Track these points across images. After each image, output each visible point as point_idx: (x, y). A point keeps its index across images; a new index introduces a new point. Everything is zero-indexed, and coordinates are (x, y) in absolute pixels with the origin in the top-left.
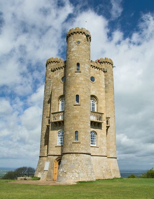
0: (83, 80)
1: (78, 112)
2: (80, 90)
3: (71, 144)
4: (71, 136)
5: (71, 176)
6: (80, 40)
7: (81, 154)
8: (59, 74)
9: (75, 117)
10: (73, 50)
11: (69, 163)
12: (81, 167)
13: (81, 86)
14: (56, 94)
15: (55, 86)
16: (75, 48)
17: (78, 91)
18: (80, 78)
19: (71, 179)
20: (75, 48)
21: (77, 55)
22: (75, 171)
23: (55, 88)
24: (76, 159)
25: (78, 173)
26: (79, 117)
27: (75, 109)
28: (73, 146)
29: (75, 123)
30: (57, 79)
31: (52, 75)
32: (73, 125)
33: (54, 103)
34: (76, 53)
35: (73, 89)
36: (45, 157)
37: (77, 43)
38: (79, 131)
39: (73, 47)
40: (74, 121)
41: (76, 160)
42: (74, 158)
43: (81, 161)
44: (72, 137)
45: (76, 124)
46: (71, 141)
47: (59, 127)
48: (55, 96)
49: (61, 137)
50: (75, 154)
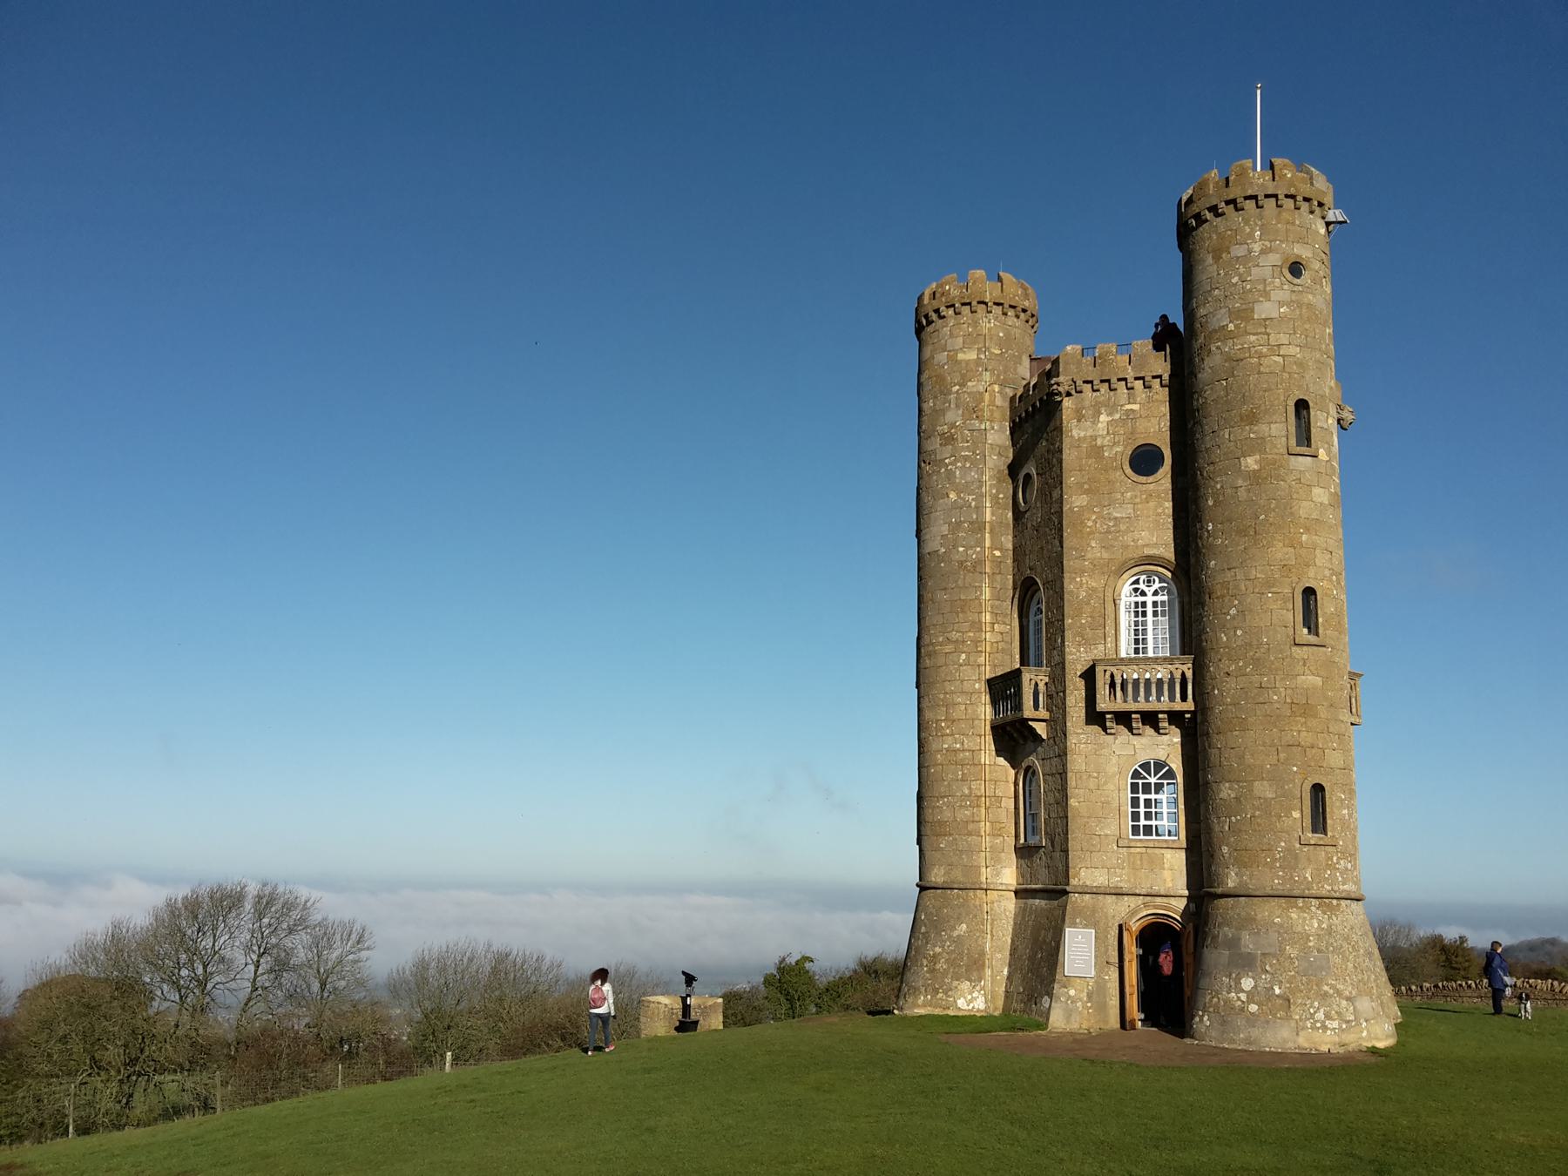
1: (1318, 681)
3: (1289, 850)
4: (1290, 809)
5: (1320, 1015)
6: (1302, 252)
7: (1343, 903)
8: (1103, 418)
9: (1303, 708)
10: (1264, 310)
13: (1320, 540)
15: (1087, 492)
16: (1280, 304)
17: (1308, 566)
18: (1316, 491)
19: (1325, 1028)
20: (1280, 304)
21: (1293, 350)
22: (1332, 987)
23: (1089, 508)
25: (1348, 999)
26: (1323, 713)
27: (1299, 668)
29: (1306, 738)
30: (1096, 451)
31: (987, 396)
34: (1284, 339)
35: (1280, 551)
41: (1330, 931)
44: (1296, 814)
49: (1153, 796)
50: (1314, 901)
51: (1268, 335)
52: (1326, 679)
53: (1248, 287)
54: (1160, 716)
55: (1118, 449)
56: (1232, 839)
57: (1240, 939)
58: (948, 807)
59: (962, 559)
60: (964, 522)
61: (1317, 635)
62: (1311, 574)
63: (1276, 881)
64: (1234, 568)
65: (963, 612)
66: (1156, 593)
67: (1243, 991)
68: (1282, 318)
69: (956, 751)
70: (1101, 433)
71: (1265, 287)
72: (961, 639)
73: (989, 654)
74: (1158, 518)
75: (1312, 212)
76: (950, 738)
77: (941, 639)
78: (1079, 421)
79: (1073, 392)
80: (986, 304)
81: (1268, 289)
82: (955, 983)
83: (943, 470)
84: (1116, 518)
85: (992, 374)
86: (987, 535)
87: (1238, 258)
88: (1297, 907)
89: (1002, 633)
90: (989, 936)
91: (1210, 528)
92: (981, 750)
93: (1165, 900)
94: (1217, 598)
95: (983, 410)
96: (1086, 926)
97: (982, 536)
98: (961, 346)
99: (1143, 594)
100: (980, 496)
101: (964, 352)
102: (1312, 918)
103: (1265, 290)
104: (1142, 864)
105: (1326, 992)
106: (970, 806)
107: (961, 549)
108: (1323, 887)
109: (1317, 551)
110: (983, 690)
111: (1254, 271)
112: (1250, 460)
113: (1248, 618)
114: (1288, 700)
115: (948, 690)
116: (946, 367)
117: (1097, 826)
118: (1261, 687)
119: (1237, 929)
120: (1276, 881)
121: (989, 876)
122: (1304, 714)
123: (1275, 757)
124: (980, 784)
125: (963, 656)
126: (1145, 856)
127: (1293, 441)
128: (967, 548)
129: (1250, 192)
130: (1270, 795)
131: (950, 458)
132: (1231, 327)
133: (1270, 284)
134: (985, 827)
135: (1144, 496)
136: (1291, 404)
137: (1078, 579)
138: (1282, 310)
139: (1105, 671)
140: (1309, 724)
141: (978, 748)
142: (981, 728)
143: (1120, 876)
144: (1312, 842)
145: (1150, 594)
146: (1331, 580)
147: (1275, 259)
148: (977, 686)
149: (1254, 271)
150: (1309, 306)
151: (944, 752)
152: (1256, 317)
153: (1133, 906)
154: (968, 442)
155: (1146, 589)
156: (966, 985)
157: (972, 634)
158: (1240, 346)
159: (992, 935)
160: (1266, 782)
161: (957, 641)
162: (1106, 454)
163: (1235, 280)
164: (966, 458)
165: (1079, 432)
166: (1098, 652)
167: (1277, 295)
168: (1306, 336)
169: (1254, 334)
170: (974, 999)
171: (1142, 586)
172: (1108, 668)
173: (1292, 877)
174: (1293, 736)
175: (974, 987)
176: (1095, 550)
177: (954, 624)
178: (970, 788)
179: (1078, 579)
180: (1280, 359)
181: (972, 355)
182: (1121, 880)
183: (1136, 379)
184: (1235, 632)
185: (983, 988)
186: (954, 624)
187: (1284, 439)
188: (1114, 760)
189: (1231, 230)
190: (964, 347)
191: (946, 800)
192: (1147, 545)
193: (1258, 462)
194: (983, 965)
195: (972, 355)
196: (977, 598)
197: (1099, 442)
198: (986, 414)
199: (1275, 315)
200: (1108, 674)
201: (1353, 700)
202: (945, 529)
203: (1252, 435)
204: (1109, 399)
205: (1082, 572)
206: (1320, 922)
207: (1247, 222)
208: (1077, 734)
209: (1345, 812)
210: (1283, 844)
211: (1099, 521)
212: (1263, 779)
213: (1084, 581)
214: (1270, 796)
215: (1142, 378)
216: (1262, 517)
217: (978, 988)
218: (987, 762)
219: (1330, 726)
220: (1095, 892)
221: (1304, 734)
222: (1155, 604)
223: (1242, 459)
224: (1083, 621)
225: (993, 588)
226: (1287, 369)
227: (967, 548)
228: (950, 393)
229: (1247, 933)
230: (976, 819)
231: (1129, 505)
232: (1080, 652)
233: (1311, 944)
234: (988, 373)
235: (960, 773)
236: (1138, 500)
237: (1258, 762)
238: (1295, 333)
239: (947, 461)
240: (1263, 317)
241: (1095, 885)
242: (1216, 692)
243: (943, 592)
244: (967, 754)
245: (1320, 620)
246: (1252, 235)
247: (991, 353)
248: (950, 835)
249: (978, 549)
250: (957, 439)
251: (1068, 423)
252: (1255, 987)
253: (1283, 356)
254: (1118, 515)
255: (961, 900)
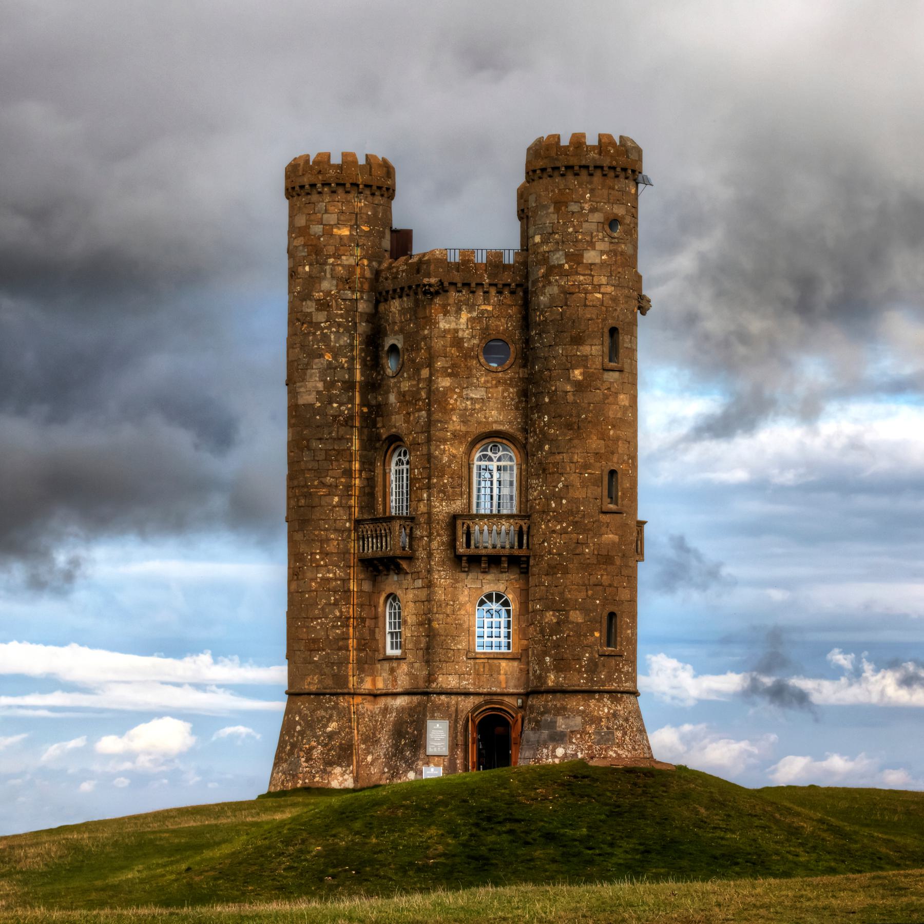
0: (627, 404)
2: (620, 451)
3: (590, 660)
7: (625, 696)
8: (464, 316)
10: (591, 256)
11: (594, 726)
12: (630, 739)
14: (454, 418)
15: (450, 375)
16: (602, 253)
17: (613, 453)
20: (602, 253)
21: (609, 289)
22: (616, 752)
23: (451, 389)
24: (612, 711)
26: (618, 561)
27: (604, 529)
28: (600, 668)
30: (457, 342)
31: (358, 270)
32: (598, 588)
33: (445, 459)
34: (604, 280)
36: (349, 694)
37: (607, 228)
38: (618, 613)
39: (592, 245)
40: (602, 575)
41: (615, 715)
42: (606, 710)
43: (627, 720)
44: (597, 634)
45: (610, 586)
46: (590, 647)
47: (481, 576)
48: (451, 427)
51: (593, 276)
52: (621, 537)
53: (580, 237)
54: (503, 559)
55: (475, 342)
56: (553, 652)
57: (556, 722)
58: (321, 626)
59: (336, 414)
60: (338, 381)
61: (616, 504)
62: (615, 460)
63: (582, 681)
64: (563, 453)
65: (337, 460)
66: (499, 460)
67: (556, 757)
68: (603, 264)
69: (329, 579)
70: (462, 327)
71: (592, 238)
72: (334, 484)
73: (358, 497)
74: (504, 400)
75: (627, 178)
76: (324, 569)
77: (316, 483)
78: (445, 315)
79: (441, 291)
80: (358, 185)
81: (594, 240)
82: (329, 769)
83: (318, 333)
84: (472, 399)
85: (362, 249)
86: (357, 394)
87: (573, 213)
88: (595, 699)
89: (367, 479)
90: (356, 732)
91: (546, 419)
92: (350, 579)
93: (500, 698)
94: (550, 474)
95: (354, 282)
96: (443, 718)
97: (353, 394)
98: (336, 222)
99: (490, 459)
100: (352, 359)
101: (339, 229)
102: (604, 706)
103: (591, 241)
104: (484, 671)
105: (611, 756)
106: (341, 626)
107: (335, 405)
108: (612, 685)
109: (620, 442)
110: (352, 528)
111: (585, 225)
112: (577, 372)
113: (571, 491)
114: (596, 553)
115: (322, 528)
116: (322, 239)
117: (451, 643)
118: (578, 543)
119: (554, 715)
120: (582, 681)
121: (355, 684)
122: (605, 563)
123: (585, 593)
124: (349, 608)
125: (336, 499)
126: (486, 664)
127: (606, 360)
128: (341, 404)
129: (583, 163)
130: (580, 620)
131: (325, 322)
132: (566, 266)
133: (595, 236)
134: (352, 643)
135: (494, 382)
136: (606, 330)
137: (442, 447)
138: (603, 258)
139: (463, 523)
140: (609, 569)
141: (348, 577)
142: (350, 560)
143: (468, 680)
144: (607, 653)
145: (495, 460)
146: (628, 463)
147: (597, 217)
148: (348, 525)
149: (585, 225)
150: (622, 253)
151: (319, 580)
152: (585, 261)
153: (476, 702)
154: (341, 309)
155: (493, 456)
156: (338, 770)
157: (343, 480)
158: (572, 283)
159: (358, 731)
160: (577, 612)
161: (330, 486)
162: (466, 345)
163: (571, 230)
164: (339, 325)
165: (445, 324)
166: (457, 506)
167: (600, 246)
168: (619, 278)
169: (584, 275)
170: (346, 780)
171: (489, 453)
172: (465, 521)
173: (592, 679)
174: (597, 578)
175: (345, 772)
176: (455, 423)
177: (328, 470)
178: (341, 612)
179: (442, 447)
180: (599, 296)
181: (345, 232)
182: (468, 684)
183: (490, 285)
184: (561, 501)
185: (352, 772)
186: (328, 470)
187: (601, 357)
188: (466, 593)
189: (569, 189)
190: (339, 224)
191: (319, 621)
192: (495, 422)
193: (583, 374)
194: (351, 754)
195: (345, 232)
196: (349, 449)
197: (460, 334)
198: (358, 285)
199: (597, 261)
200: (465, 526)
201: (639, 542)
202: (320, 386)
203: (578, 353)
204: (469, 299)
205: (445, 441)
206: (609, 709)
207: (580, 185)
208: (439, 571)
209: (629, 631)
210: (587, 655)
211: (459, 400)
212: (576, 609)
213: (447, 449)
214: (581, 621)
215: (496, 285)
216: (583, 416)
217: (348, 772)
218: (355, 590)
219: (622, 571)
220: (449, 693)
221: (605, 577)
222: (499, 469)
223: (571, 371)
224: (446, 481)
225: (361, 440)
226: (605, 304)
227: (341, 404)
228: (325, 263)
229: (561, 717)
230: (346, 636)
231: (482, 389)
232: (442, 505)
233: (602, 724)
234: (359, 249)
235: (332, 598)
236: (489, 385)
237: (573, 597)
238: (611, 276)
239: (322, 325)
240: (590, 262)
241: (449, 687)
242: (546, 544)
243: (318, 442)
244: (339, 582)
245: (620, 494)
246: (583, 197)
247: (362, 231)
248: (324, 650)
249: (350, 406)
250: (332, 305)
251: (436, 316)
252: (566, 754)
253: (603, 294)
254: (474, 396)
255: (333, 703)
